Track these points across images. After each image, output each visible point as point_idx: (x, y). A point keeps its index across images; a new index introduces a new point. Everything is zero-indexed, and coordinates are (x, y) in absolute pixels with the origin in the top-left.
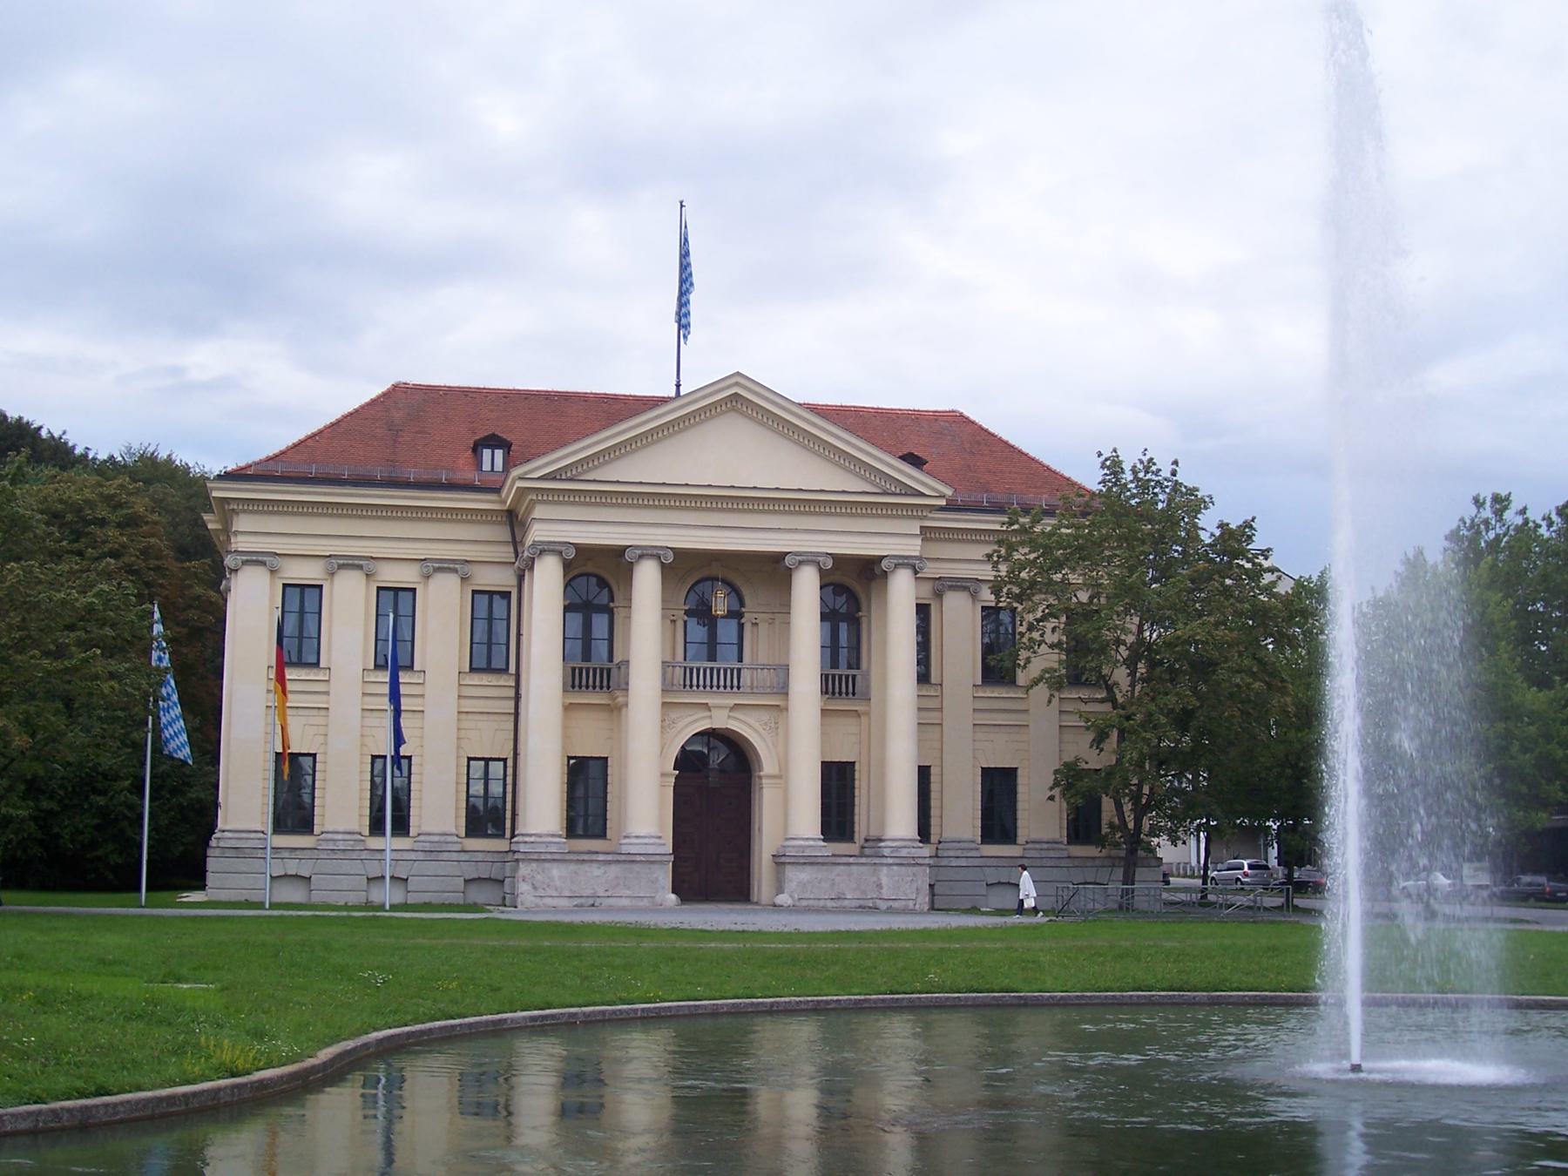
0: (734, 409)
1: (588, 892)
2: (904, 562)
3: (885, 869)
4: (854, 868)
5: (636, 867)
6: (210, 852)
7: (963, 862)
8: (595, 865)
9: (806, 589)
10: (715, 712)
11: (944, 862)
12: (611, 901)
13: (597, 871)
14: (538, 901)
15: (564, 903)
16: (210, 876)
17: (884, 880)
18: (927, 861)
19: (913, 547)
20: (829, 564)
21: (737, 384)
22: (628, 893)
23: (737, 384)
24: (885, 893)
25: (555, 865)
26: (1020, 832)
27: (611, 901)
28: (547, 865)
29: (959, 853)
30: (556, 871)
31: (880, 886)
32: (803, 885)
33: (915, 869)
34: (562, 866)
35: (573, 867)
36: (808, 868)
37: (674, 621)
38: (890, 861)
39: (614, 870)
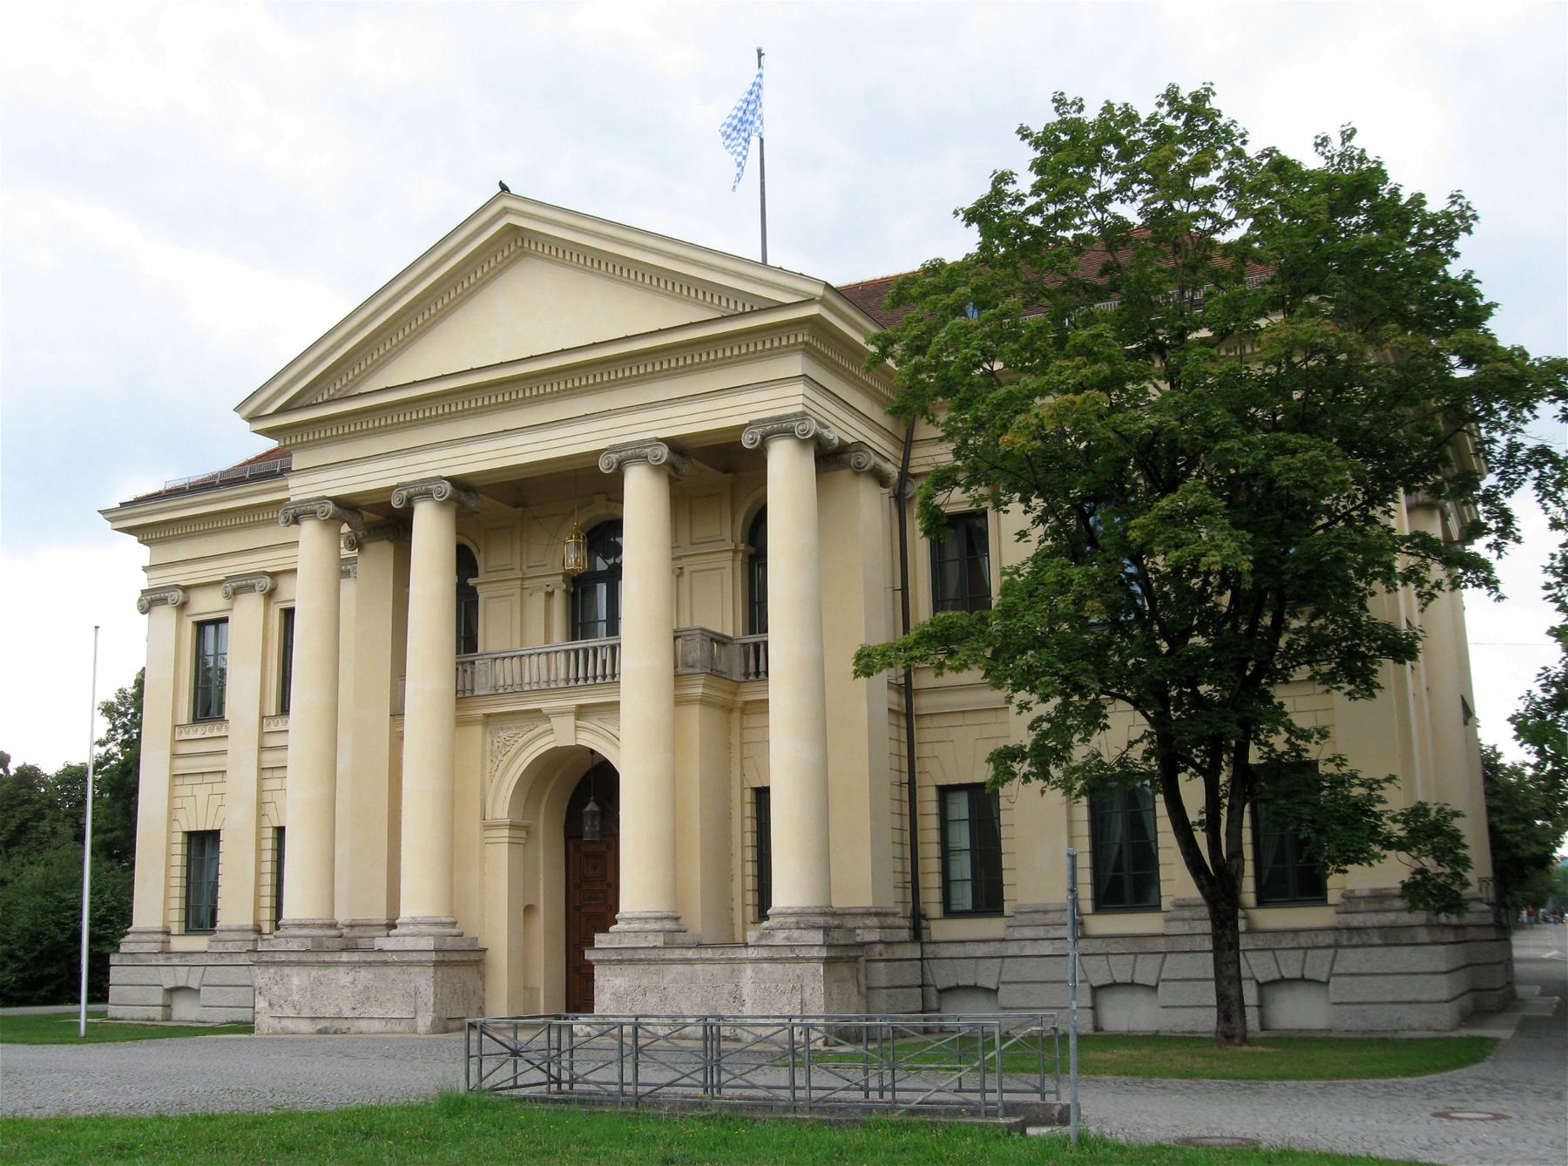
0: (524, 254)
1: (330, 1011)
2: (780, 428)
3: (749, 970)
4: (699, 967)
5: (391, 972)
6: (114, 959)
7: (1047, 948)
8: (342, 970)
9: (643, 504)
10: (556, 722)
11: (1013, 949)
12: (363, 1025)
13: (343, 977)
14: (275, 1022)
15: (305, 1026)
16: (112, 991)
17: (747, 989)
18: (815, 953)
19: (788, 400)
20: (664, 451)
21: (505, 211)
22: (379, 1012)
23: (505, 211)
24: (747, 1011)
25: (295, 970)
26: (1165, 888)
27: (363, 1025)
28: (286, 970)
29: (1041, 932)
30: (297, 979)
31: (737, 998)
32: (617, 997)
33: (798, 968)
34: (304, 971)
35: (315, 972)
36: (629, 970)
37: (550, 595)
38: (752, 953)
39: (365, 975)
